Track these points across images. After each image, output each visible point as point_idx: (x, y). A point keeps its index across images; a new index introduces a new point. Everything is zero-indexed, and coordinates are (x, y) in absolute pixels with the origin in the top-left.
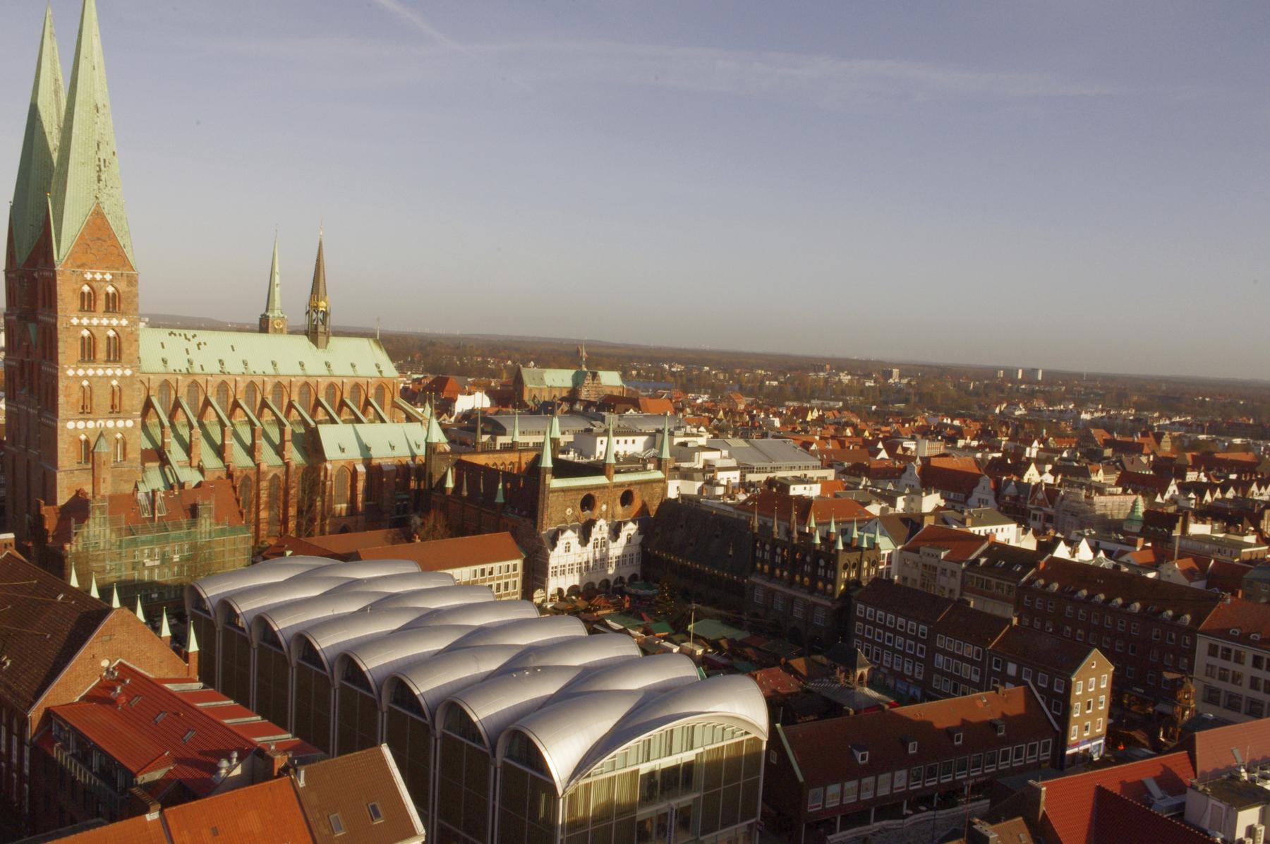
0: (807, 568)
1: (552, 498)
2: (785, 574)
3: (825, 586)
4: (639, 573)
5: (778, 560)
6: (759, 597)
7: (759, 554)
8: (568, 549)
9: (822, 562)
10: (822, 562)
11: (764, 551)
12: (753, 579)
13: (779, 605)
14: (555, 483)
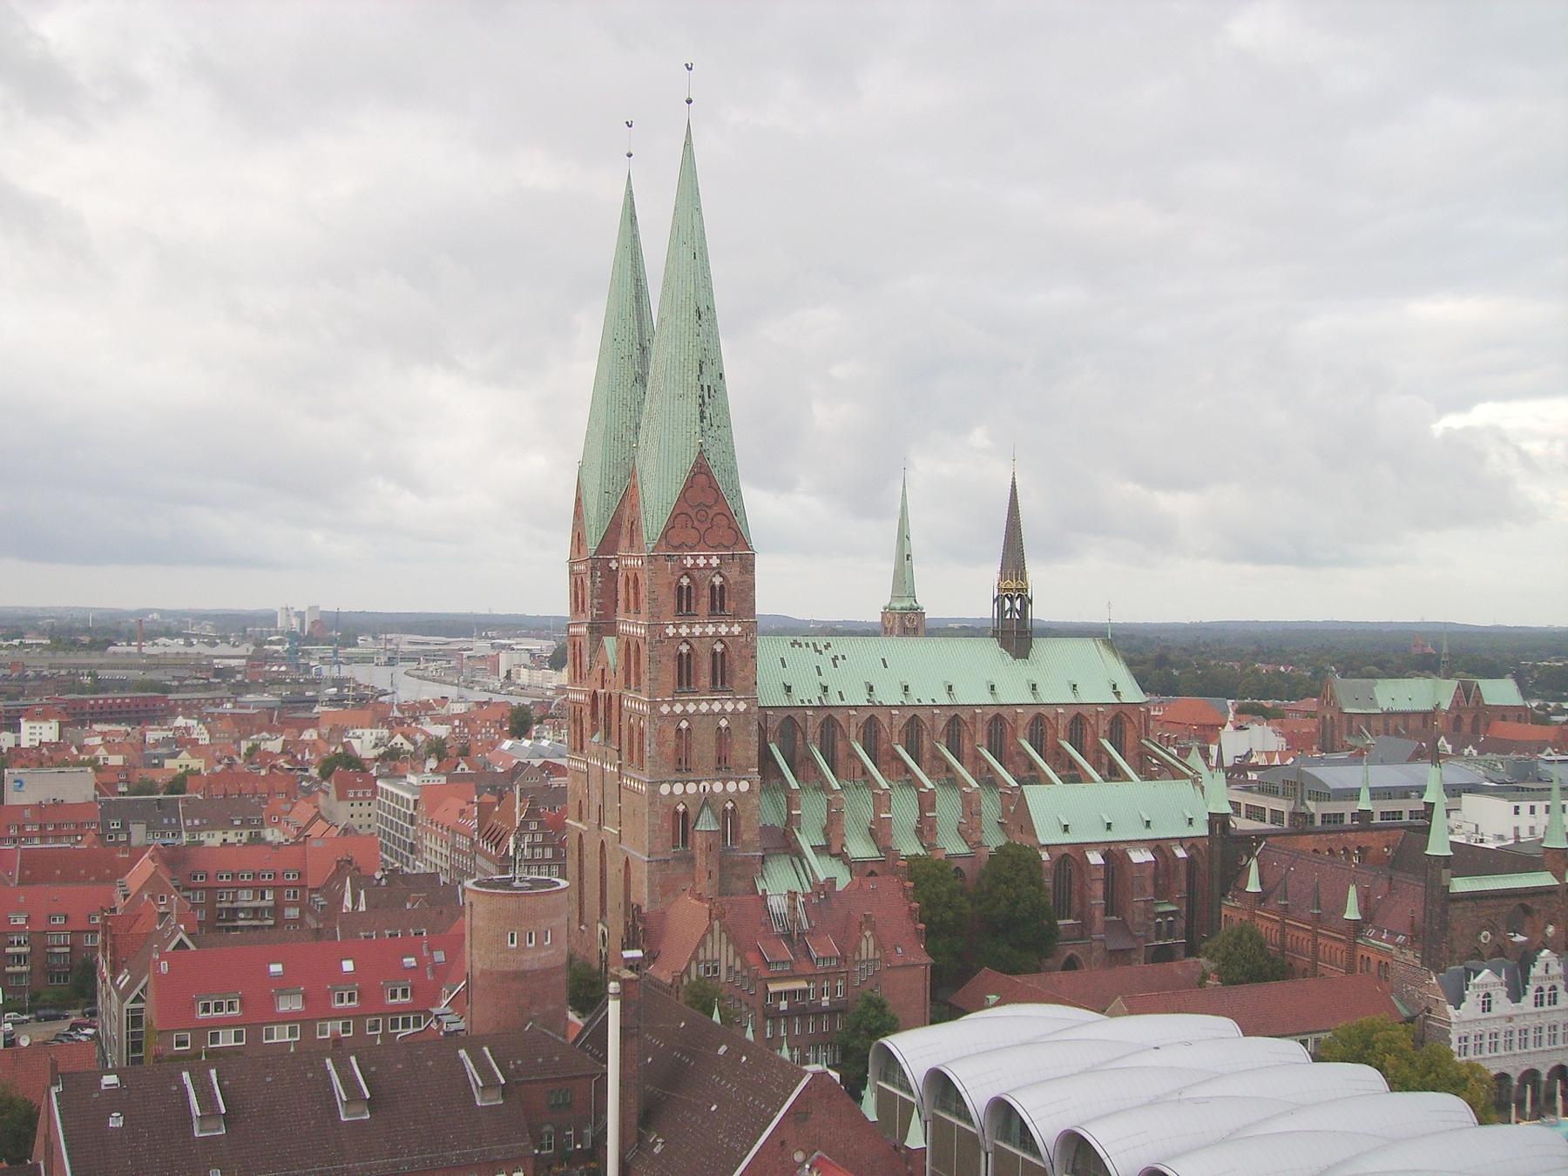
8: (1487, 1006)
14: (1461, 885)
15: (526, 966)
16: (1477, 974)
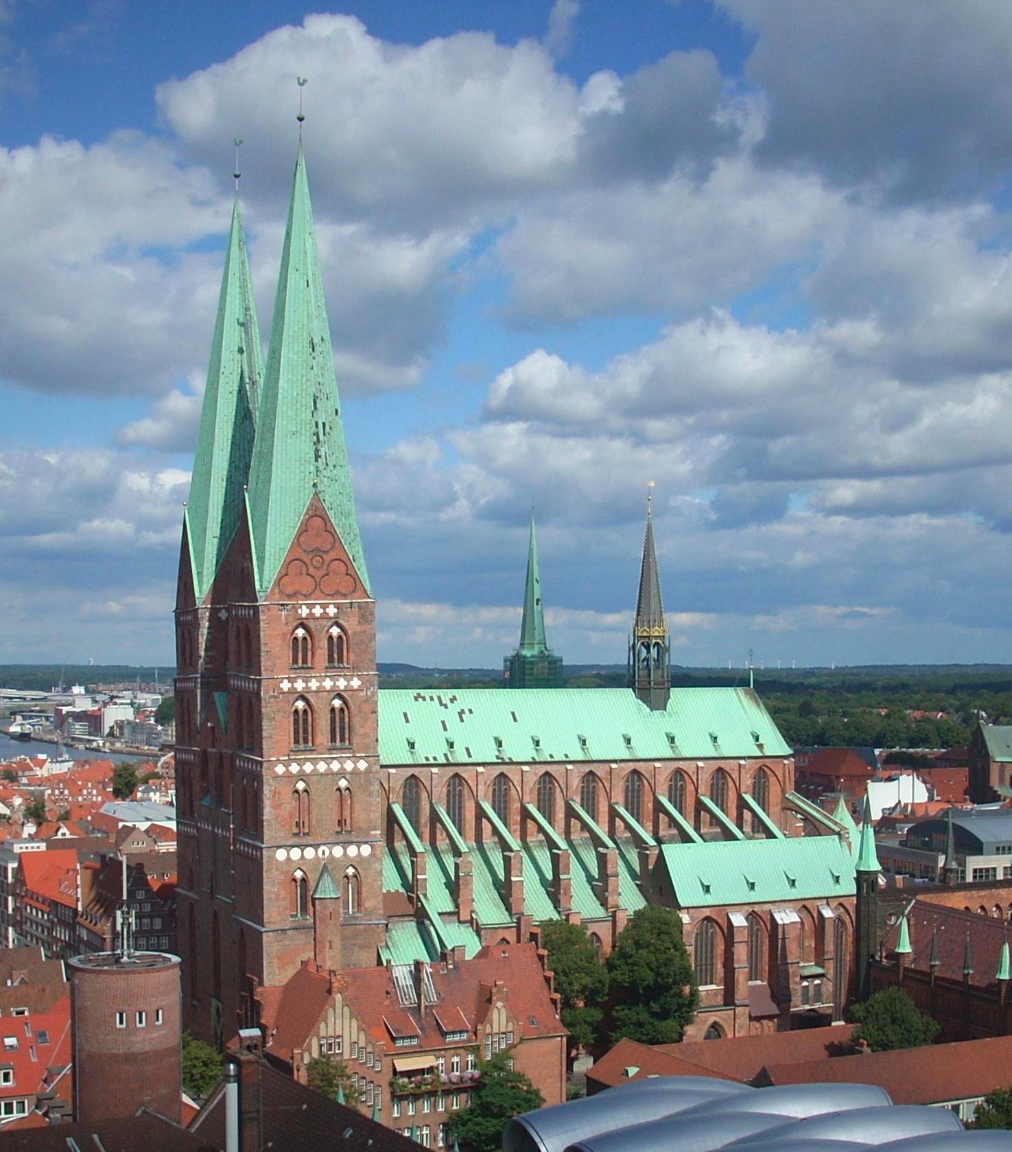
15: (137, 1048)
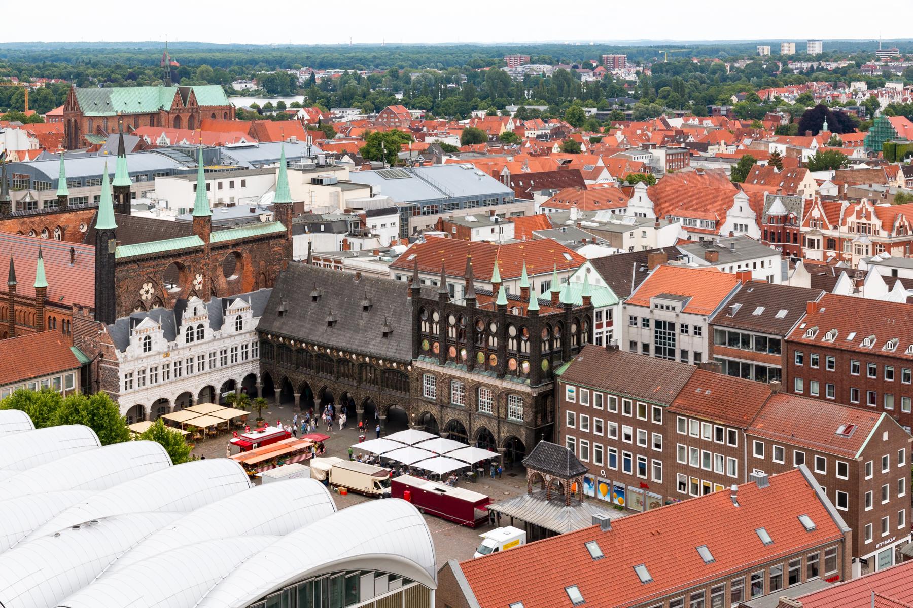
0: (493, 342)
1: (119, 273)
2: (464, 353)
3: (520, 364)
4: (257, 372)
5: (452, 333)
6: (429, 389)
7: (425, 327)
8: (147, 346)
9: (513, 331)
10: (513, 331)
11: (430, 320)
12: (418, 364)
13: (457, 397)
14: (124, 252)
16: (138, 321)
